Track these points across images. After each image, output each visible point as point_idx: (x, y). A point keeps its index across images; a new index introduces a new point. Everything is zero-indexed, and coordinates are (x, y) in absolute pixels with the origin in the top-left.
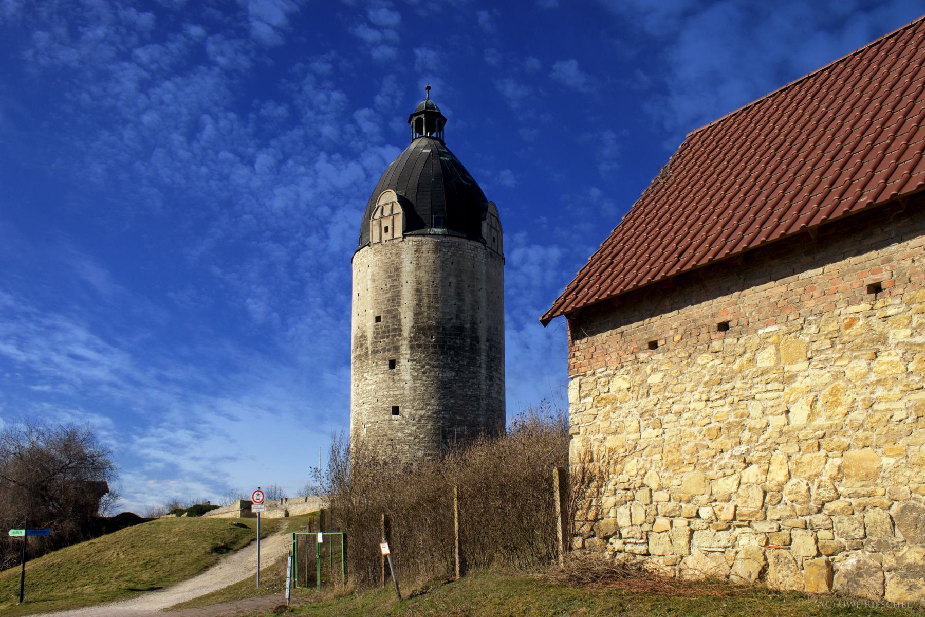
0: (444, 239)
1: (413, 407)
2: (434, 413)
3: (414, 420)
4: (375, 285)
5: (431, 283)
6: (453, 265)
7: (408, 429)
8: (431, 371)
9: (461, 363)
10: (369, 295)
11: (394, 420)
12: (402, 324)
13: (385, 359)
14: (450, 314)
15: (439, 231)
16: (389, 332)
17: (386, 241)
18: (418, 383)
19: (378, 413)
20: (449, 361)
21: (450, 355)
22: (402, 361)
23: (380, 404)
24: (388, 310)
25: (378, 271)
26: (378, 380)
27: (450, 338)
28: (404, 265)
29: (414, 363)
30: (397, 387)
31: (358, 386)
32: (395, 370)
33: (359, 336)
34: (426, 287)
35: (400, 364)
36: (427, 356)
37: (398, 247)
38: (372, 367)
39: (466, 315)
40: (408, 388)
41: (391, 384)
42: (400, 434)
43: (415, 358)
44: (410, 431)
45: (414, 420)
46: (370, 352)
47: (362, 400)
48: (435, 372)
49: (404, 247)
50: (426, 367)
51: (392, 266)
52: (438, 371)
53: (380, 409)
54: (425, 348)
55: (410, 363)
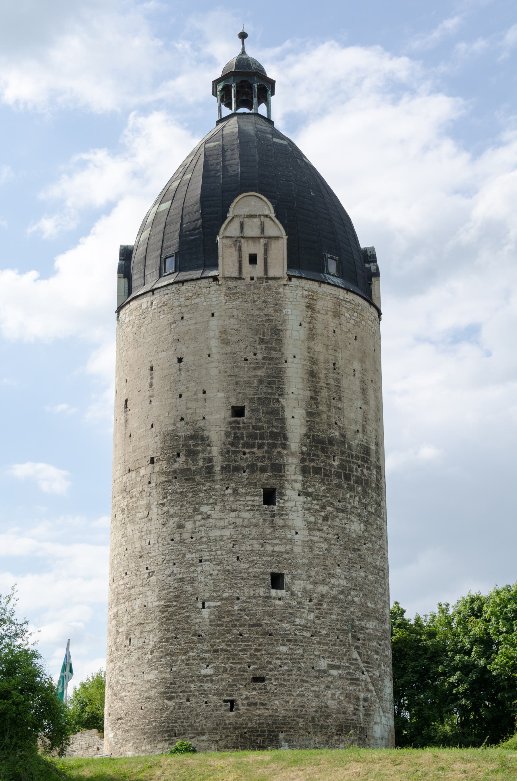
0: (346, 296)
1: (309, 577)
2: (342, 592)
3: (310, 601)
4: (229, 349)
5: (332, 365)
7: (301, 618)
8: (335, 517)
10: (213, 365)
11: (275, 598)
12: (288, 427)
13: (255, 485)
16: (262, 437)
17: (252, 279)
18: (316, 536)
20: (356, 504)
21: (358, 492)
22: (288, 492)
24: (259, 399)
25: (236, 327)
26: (239, 521)
28: (289, 327)
29: (309, 499)
30: (281, 539)
31: (180, 526)
32: (275, 507)
35: (286, 498)
37: (277, 293)
38: (224, 495)
40: (300, 543)
41: (268, 531)
42: (286, 625)
43: (310, 490)
44: (304, 622)
45: (310, 601)
46: (217, 469)
47: (198, 555)
48: (341, 520)
49: (289, 295)
50: (328, 509)
51: (267, 324)
52: (344, 518)
53: (245, 576)
54: (325, 475)
55: (302, 498)
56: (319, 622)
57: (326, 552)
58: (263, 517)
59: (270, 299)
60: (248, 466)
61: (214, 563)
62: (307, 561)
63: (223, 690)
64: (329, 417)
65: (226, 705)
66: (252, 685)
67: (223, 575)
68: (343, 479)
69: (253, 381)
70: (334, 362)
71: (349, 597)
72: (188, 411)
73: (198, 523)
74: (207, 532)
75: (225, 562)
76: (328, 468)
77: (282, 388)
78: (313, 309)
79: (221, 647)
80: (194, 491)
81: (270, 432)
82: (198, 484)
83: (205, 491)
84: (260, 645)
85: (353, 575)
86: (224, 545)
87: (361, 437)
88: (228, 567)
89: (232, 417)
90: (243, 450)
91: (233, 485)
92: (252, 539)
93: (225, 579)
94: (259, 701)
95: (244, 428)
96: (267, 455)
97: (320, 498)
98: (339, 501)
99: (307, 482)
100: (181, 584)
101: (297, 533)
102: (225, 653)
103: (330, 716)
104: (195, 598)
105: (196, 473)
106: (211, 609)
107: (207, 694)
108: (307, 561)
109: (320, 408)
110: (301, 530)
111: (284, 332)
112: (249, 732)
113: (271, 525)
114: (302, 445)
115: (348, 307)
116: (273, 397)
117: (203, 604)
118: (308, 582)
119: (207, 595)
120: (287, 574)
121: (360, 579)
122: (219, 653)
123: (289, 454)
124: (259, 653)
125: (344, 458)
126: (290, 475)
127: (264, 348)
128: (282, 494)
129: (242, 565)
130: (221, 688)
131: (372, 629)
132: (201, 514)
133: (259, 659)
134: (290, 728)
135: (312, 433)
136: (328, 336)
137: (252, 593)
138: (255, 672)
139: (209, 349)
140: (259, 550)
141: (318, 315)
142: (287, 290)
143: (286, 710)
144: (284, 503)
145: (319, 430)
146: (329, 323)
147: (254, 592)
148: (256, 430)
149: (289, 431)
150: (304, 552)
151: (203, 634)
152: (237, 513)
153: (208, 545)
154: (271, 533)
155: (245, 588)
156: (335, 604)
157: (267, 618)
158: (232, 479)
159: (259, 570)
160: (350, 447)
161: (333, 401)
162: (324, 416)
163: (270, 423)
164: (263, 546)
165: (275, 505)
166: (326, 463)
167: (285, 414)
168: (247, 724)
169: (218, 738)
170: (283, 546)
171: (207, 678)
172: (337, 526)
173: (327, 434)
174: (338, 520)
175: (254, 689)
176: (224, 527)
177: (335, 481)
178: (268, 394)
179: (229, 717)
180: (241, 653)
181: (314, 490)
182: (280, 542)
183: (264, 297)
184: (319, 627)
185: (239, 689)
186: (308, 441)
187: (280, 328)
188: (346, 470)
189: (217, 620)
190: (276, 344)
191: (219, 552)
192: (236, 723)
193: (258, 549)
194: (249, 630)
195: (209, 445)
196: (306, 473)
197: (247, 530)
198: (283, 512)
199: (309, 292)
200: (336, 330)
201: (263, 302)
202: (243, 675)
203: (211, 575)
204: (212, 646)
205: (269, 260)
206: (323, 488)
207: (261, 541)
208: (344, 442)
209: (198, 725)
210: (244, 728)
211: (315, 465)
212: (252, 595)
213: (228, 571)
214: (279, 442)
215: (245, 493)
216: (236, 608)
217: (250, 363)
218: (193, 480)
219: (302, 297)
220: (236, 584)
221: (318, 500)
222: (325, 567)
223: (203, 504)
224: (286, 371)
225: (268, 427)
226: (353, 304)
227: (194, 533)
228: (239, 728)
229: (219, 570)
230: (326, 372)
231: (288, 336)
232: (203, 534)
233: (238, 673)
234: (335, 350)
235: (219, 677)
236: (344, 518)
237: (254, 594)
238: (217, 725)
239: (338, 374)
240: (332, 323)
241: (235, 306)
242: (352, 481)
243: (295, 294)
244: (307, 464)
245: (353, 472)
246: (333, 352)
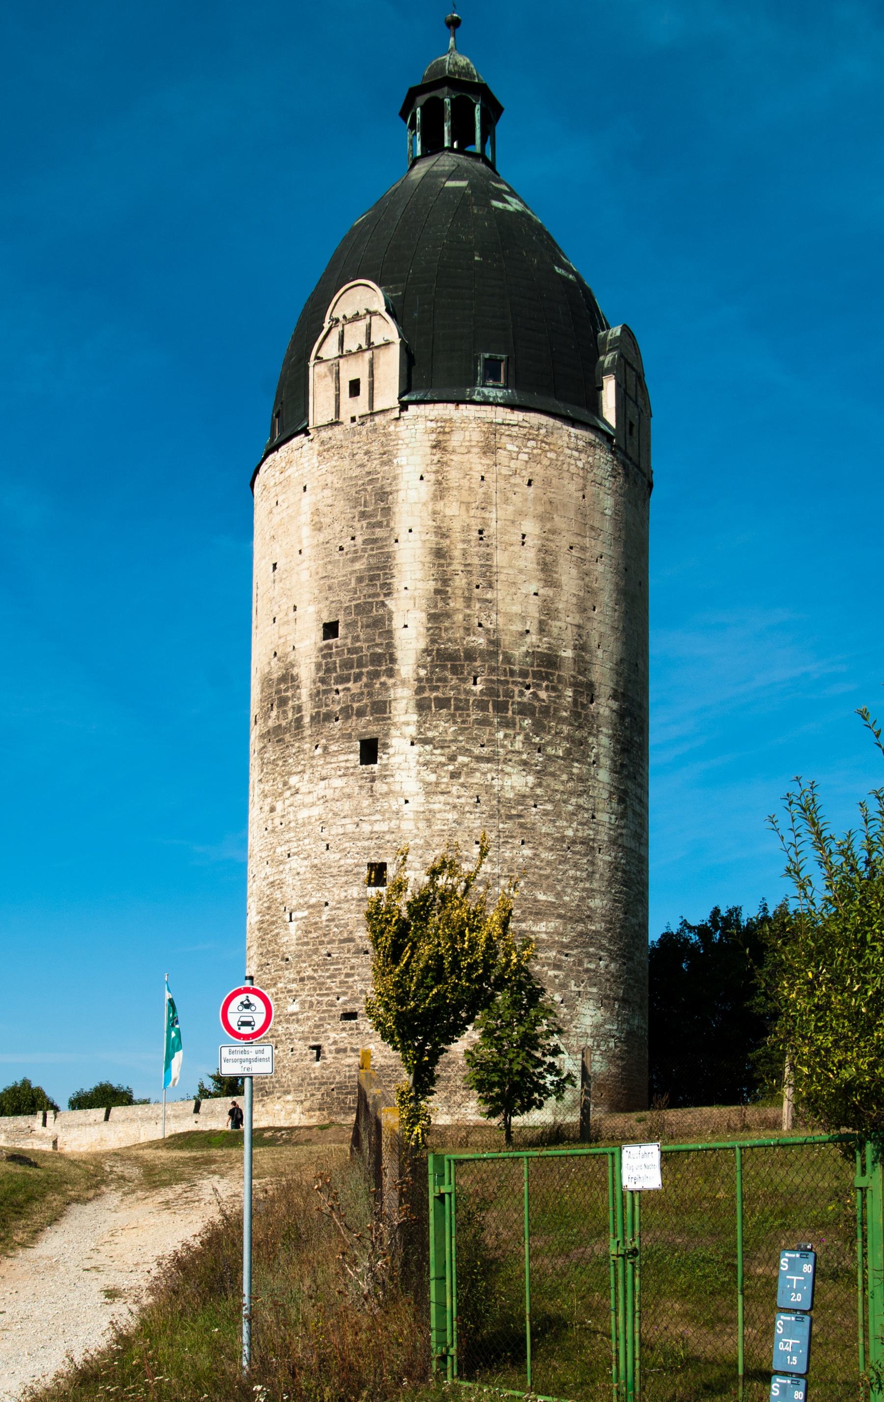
5: (476, 534)
6: (532, 489)
8: (473, 771)
9: (550, 750)
12: (397, 642)
13: (349, 737)
14: (523, 618)
15: (492, 393)
16: (360, 665)
17: (353, 419)
18: (438, 803)
19: (329, 882)
20: (518, 746)
21: (521, 727)
23: (332, 856)
24: (356, 606)
26: (329, 793)
27: (522, 684)
28: (402, 484)
29: (428, 748)
32: (375, 767)
33: (275, 676)
34: (460, 546)
35: (391, 751)
36: (462, 731)
37: (385, 435)
38: (313, 758)
39: (563, 625)
40: (411, 815)
41: (365, 803)
43: (430, 734)
46: (307, 720)
47: (285, 848)
48: (484, 774)
50: (461, 759)
51: (369, 488)
52: (490, 770)
53: (335, 871)
54: (457, 708)
55: (417, 748)
57: (454, 825)
59: (375, 448)
60: (342, 710)
61: (302, 856)
62: (422, 842)
63: (309, 1032)
64: (467, 617)
65: (312, 1053)
66: (341, 1024)
68: (491, 710)
69: (350, 580)
70: (480, 527)
71: (497, 889)
75: (313, 854)
76: (462, 697)
77: (390, 584)
78: (444, 449)
79: (307, 974)
84: (352, 968)
85: (506, 855)
87: (534, 640)
88: (316, 862)
89: (325, 638)
90: (335, 687)
91: (323, 741)
93: (313, 879)
94: (349, 1046)
96: (366, 690)
97: (446, 745)
98: (482, 746)
99: (425, 723)
101: (407, 802)
102: (312, 981)
103: (453, 1062)
107: (293, 1040)
108: (422, 842)
109: (452, 605)
110: (413, 795)
111: (395, 495)
112: (338, 1088)
113: (370, 794)
114: (419, 666)
115: (514, 434)
116: (376, 599)
117: (291, 914)
119: (294, 903)
121: (521, 860)
122: (306, 983)
123: (398, 683)
124: (351, 979)
125: (495, 678)
126: (399, 715)
127: (365, 525)
128: (386, 746)
129: (332, 856)
130: (307, 1030)
131: (546, 933)
133: (351, 987)
134: (390, 1081)
135: (436, 646)
136: (470, 488)
137: (343, 894)
138: (345, 1007)
140: (353, 833)
141: (452, 457)
143: (385, 1057)
144: (388, 758)
145: (449, 640)
146: (473, 465)
147: (345, 894)
148: (352, 654)
149: (399, 648)
151: (290, 958)
152: (326, 781)
154: (369, 805)
155: (334, 889)
160: (508, 659)
161: (476, 591)
162: (459, 617)
165: (375, 762)
167: (394, 622)
168: (334, 1078)
169: (303, 1098)
170: (386, 823)
171: (294, 1017)
173: (463, 645)
175: (344, 1029)
176: (313, 804)
177: (475, 714)
178: (370, 596)
179: (314, 1069)
180: (329, 981)
181: (437, 734)
183: (366, 444)
185: (325, 1031)
186: (429, 659)
187: (388, 490)
188: (498, 696)
190: (383, 516)
191: (307, 841)
192: (323, 1077)
193: (351, 831)
196: (423, 710)
197: (337, 806)
198: (387, 773)
200: (486, 476)
201: (366, 454)
202: (330, 1011)
203: (298, 874)
204: (299, 973)
205: (376, 385)
206: (452, 729)
207: (356, 819)
208: (497, 654)
209: (284, 1080)
210: (331, 1083)
212: (343, 898)
213: (316, 866)
214: (384, 668)
217: (347, 554)
219: (426, 433)
220: (324, 884)
221: (442, 748)
224: (397, 557)
225: (369, 647)
226: (525, 427)
228: (325, 1083)
229: (306, 867)
230: (465, 546)
231: (400, 500)
232: (291, 817)
233: (325, 1008)
234: (483, 509)
235: (305, 1014)
238: (303, 1080)
239: (488, 546)
240: (478, 464)
242: (510, 712)
243: (413, 431)
244: (426, 695)
245: (512, 697)
246: (479, 513)
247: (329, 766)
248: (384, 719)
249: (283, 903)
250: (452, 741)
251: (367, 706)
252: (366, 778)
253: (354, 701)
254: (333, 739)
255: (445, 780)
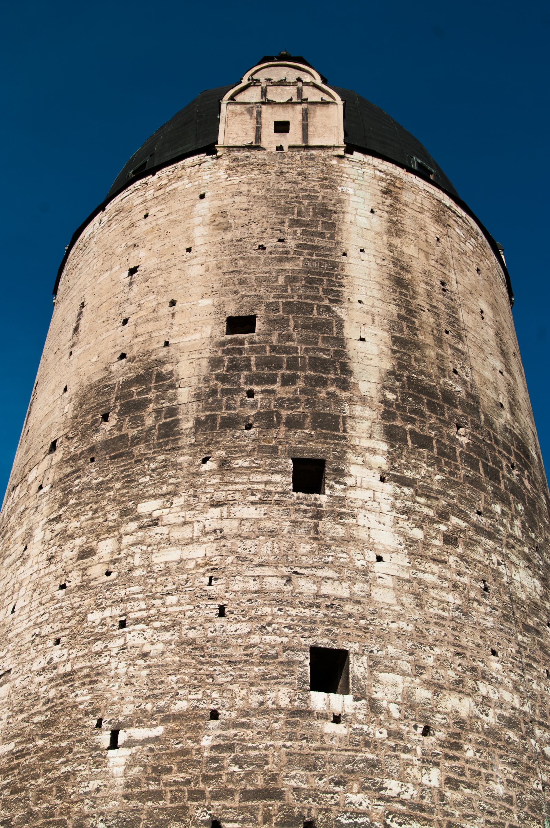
1: (419, 669)
2: (511, 723)
3: (426, 732)
4: (229, 236)
7: (403, 779)
11: (323, 716)
12: (351, 354)
13: (274, 451)
22: (353, 470)
24: (285, 304)
25: (245, 206)
26: (230, 527)
30: (339, 569)
32: (323, 499)
35: (349, 481)
38: (198, 474)
43: (408, 474)
45: (426, 732)
46: (187, 425)
47: (117, 611)
52: (494, 551)
53: (238, 654)
54: (441, 453)
55: (389, 487)
56: (458, 796)
58: (293, 517)
60: (258, 416)
61: (157, 624)
67: (176, 654)
72: (136, 340)
73: (127, 540)
74: (147, 558)
77: (338, 292)
80: (129, 476)
81: (311, 358)
82: (138, 461)
83: (153, 470)
85: (534, 686)
86: (187, 581)
88: (192, 634)
92: (261, 565)
95: (252, 350)
96: (303, 398)
98: (479, 513)
99: (399, 456)
100: (64, 688)
101: (379, 559)
104: (95, 722)
105: (136, 440)
106: (134, 750)
113: (312, 534)
114: (384, 387)
117: (115, 735)
118: (417, 680)
119: (128, 709)
120: (357, 654)
126: (360, 438)
128: (340, 473)
129: (231, 628)
132: (138, 518)
137: (255, 700)
139: (190, 239)
140: (280, 592)
141: (406, 209)
142: (345, 164)
147: (261, 698)
149: (355, 360)
150: (402, 605)
152: (225, 508)
153: (146, 584)
155: (235, 688)
156: (497, 751)
157: (300, 772)
158: (217, 442)
159: (279, 640)
163: (311, 343)
164: (289, 581)
166: (441, 432)
167: (345, 331)
172: (480, 562)
174: (480, 550)
176: (192, 541)
178: (307, 297)
182: (335, 575)
184: (457, 813)
189: (148, 779)
191: (172, 599)
193: (275, 588)
194: (241, 810)
195: (172, 386)
196: (396, 440)
199: (387, 174)
203: (145, 655)
205: (311, 129)
206: (438, 477)
207: (286, 571)
208: (477, 409)
211: (418, 430)
212: (254, 705)
213: (192, 642)
214: (333, 377)
215: (247, 468)
216: (206, 742)
218: (129, 454)
220: (211, 676)
221: (428, 497)
222: (459, 650)
223: (146, 498)
224: (347, 268)
225: (306, 350)
227: (114, 562)
229: (169, 643)
236: (494, 551)
237: (262, 704)
241: (245, 180)
244: (398, 423)
247: (233, 487)
248: (335, 437)
249: (95, 711)
250: (440, 493)
251: (305, 416)
252: (305, 511)
253: (283, 407)
254: (241, 452)
255: (437, 542)
